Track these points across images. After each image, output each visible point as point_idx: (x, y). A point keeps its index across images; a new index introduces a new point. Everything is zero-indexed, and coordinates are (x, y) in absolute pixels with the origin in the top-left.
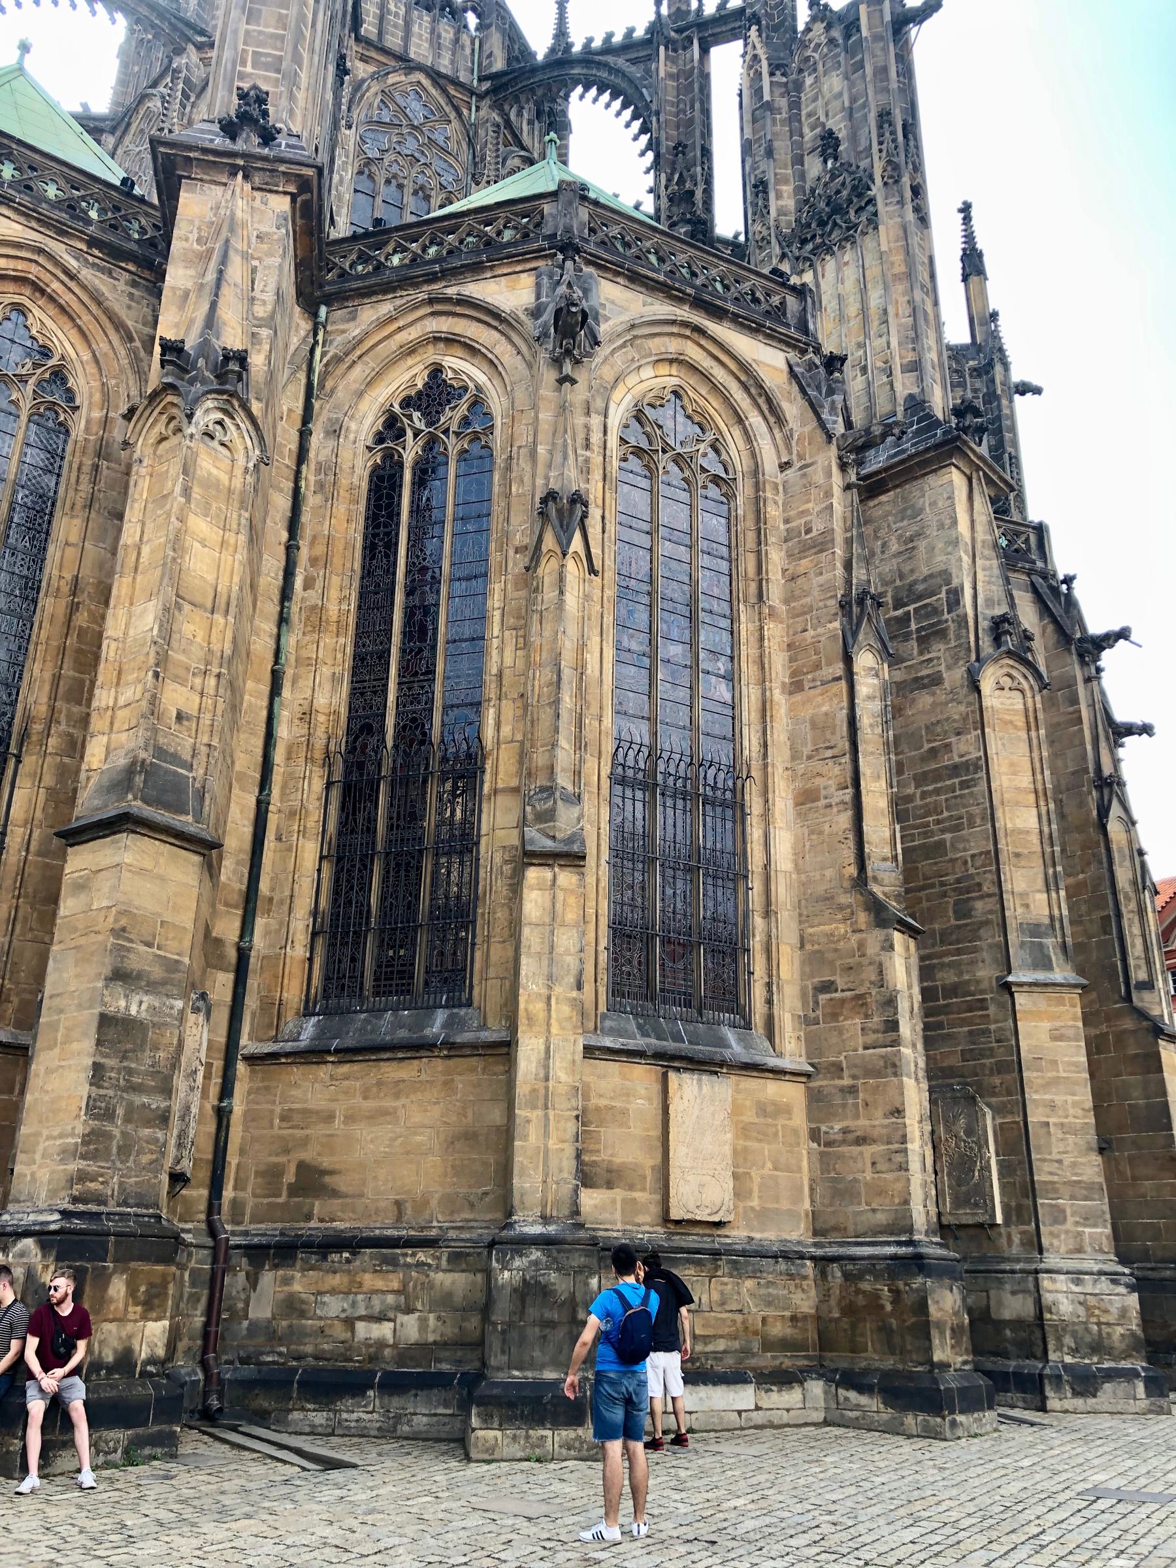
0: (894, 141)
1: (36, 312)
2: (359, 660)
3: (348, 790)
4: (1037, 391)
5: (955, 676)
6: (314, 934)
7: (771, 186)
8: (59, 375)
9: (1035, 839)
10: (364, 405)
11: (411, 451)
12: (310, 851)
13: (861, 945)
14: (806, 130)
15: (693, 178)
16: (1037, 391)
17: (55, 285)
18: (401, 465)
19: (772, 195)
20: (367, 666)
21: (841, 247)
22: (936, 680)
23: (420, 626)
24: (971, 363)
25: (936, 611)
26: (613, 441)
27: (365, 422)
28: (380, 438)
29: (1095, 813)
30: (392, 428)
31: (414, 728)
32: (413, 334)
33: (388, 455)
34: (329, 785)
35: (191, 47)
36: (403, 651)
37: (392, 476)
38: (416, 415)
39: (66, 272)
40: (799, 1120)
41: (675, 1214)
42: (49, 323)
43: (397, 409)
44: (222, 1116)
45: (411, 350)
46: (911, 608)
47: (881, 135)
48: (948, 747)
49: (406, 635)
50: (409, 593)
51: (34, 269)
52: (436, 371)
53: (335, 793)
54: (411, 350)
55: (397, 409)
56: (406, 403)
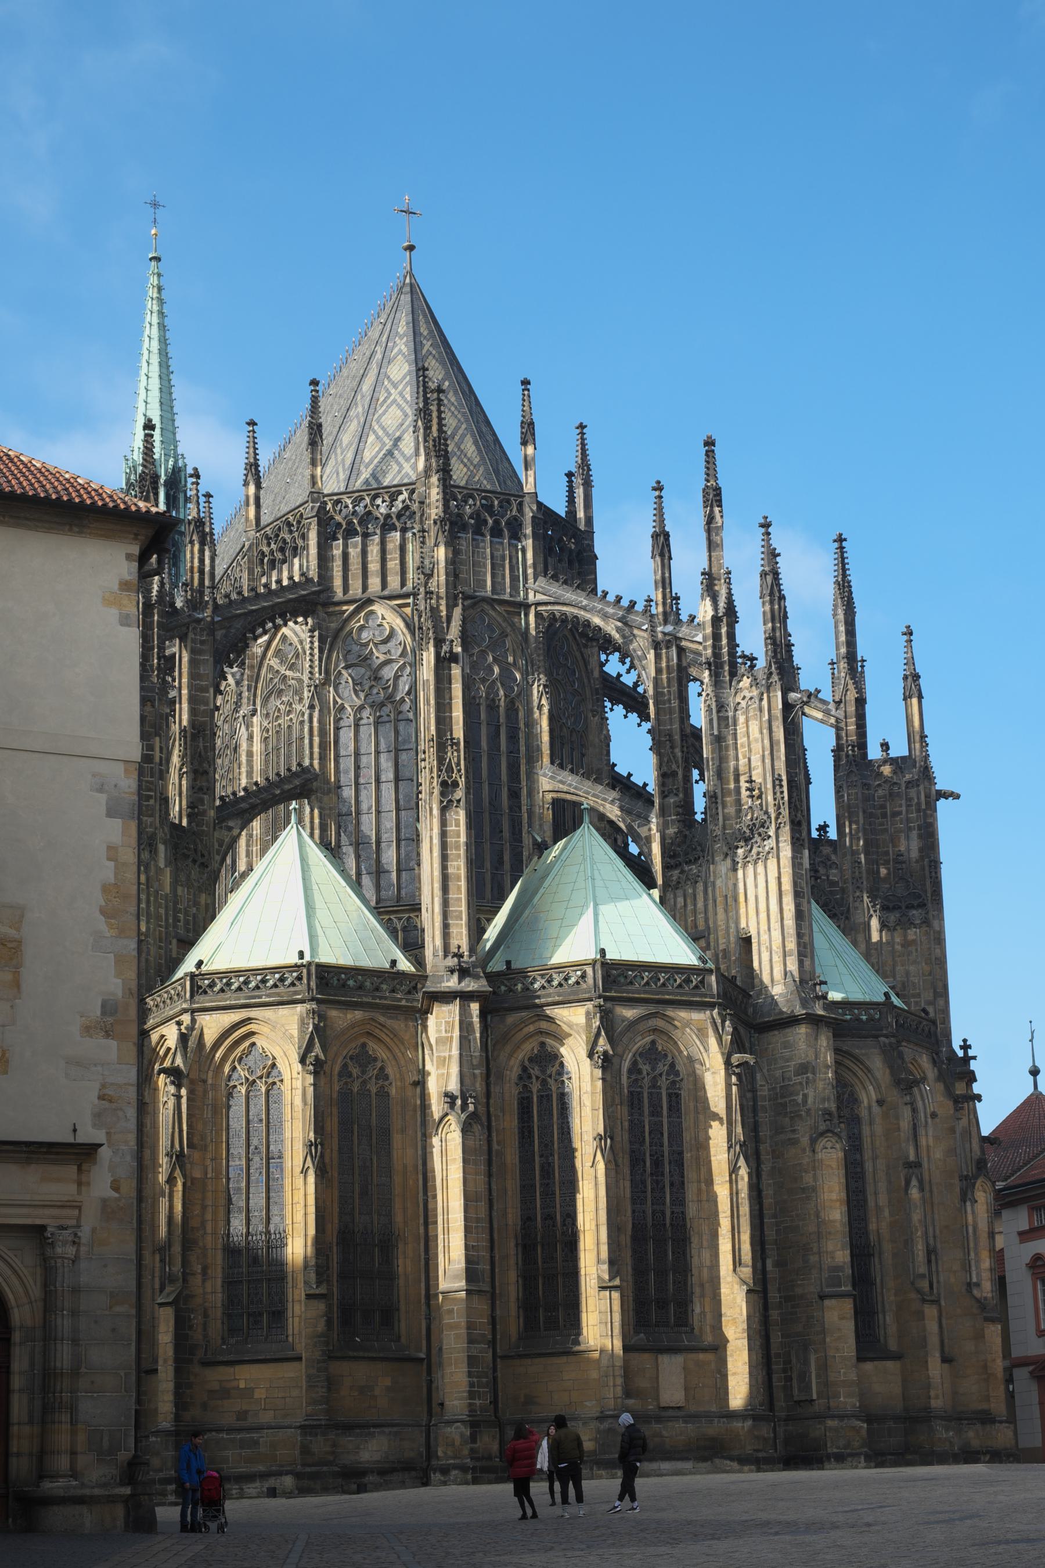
0: (783, 798)
1: (370, 1043)
2: (523, 1187)
3: (524, 1247)
4: (957, 797)
5: (805, 1140)
6: (519, 1308)
7: (719, 801)
8: (382, 1069)
9: (838, 1225)
10: (512, 1063)
11: (535, 1087)
12: (512, 1276)
13: (735, 1299)
14: (740, 756)
15: (677, 762)
16: (957, 797)
17: (377, 1031)
18: (531, 1092)
19: (720, 808)
20: (527, 1189)
21: (756, 863)
22: (794, 1142)
23: (547, 1172)
24: (908, 777)
25: (798, 1104)
26: (624, 1080)
27: (513, 1072)
28: (520, 1078)
29: (903, 1183)
30: (525, 1075)
31: (549, 1217)
32: (531, 1028)
33: (525, 1086)
34: (517, 1245)
35: (319, 607)
36: (541, 1185)
37: (528, 1097)
38: (536, 1068)
39: (380, 1024)
40: (713, 1366)
41: (662, 1405)
42: (375, 1047)
43: (527, 1063)
44: (495, 1379)
45: (530, 1036)
46: (787, 1100)
47: (775, 793)
48: (802, 1177)
49: (542, 1177)
50: (541, 1156)
51: (368, 1026)
52: (543, 1044)
53: (520, 1249)
54: (530, 1036)
55: (527, 1063)
56: (531, 1060)
